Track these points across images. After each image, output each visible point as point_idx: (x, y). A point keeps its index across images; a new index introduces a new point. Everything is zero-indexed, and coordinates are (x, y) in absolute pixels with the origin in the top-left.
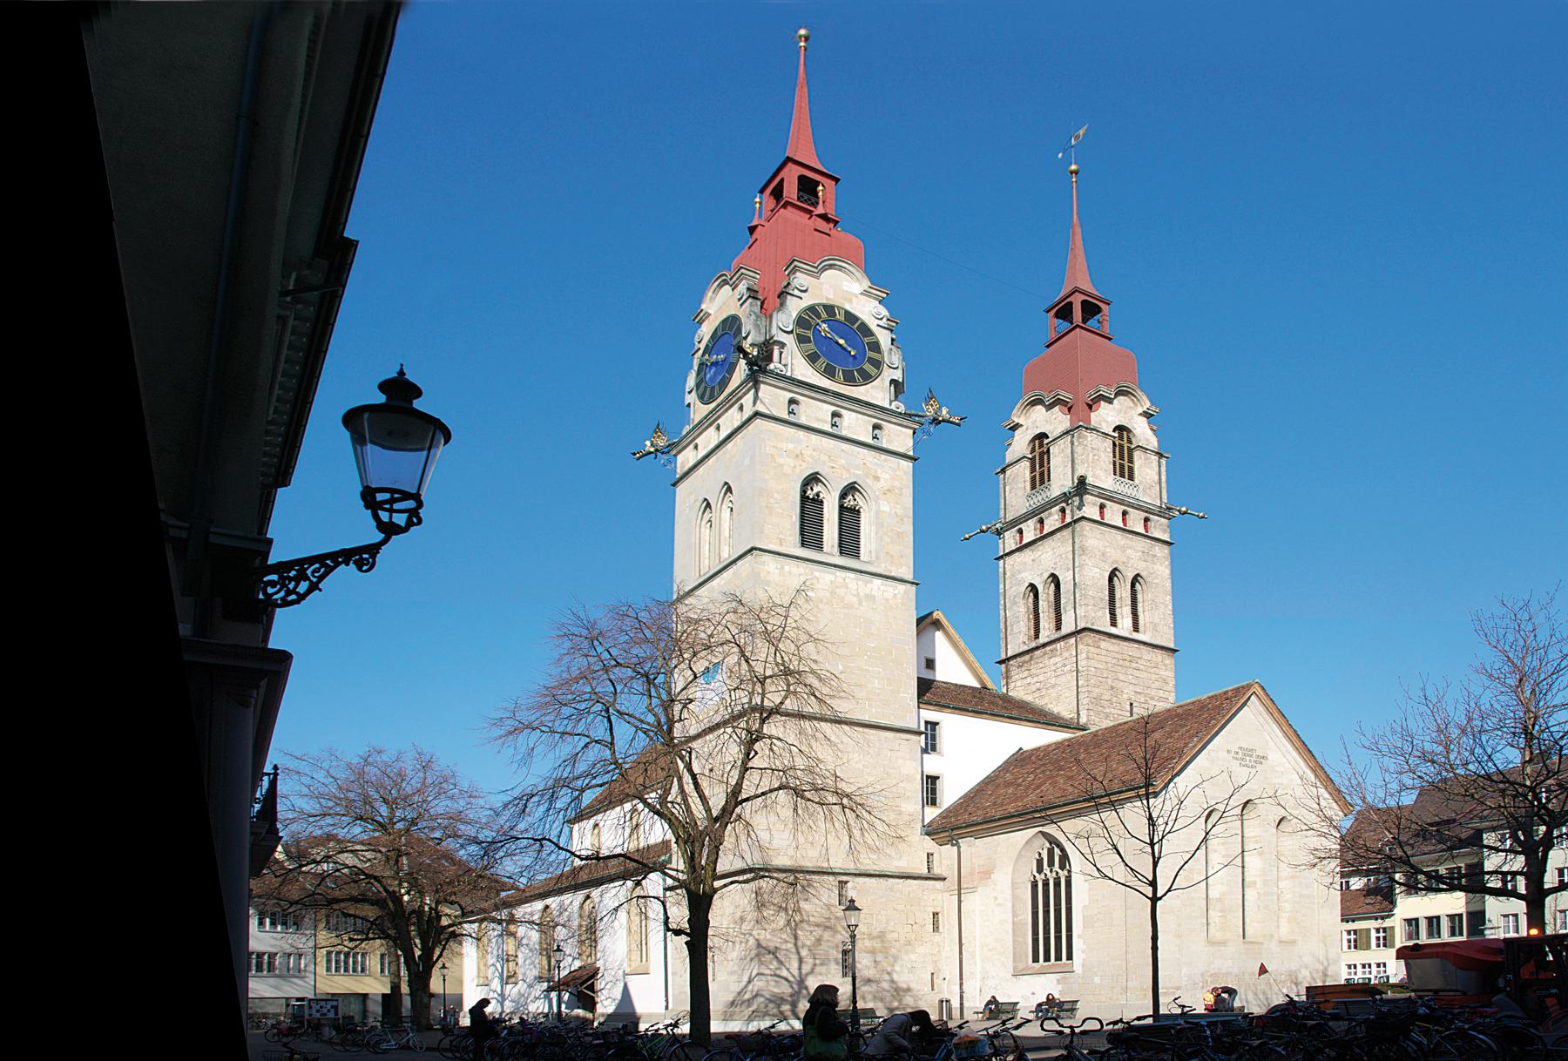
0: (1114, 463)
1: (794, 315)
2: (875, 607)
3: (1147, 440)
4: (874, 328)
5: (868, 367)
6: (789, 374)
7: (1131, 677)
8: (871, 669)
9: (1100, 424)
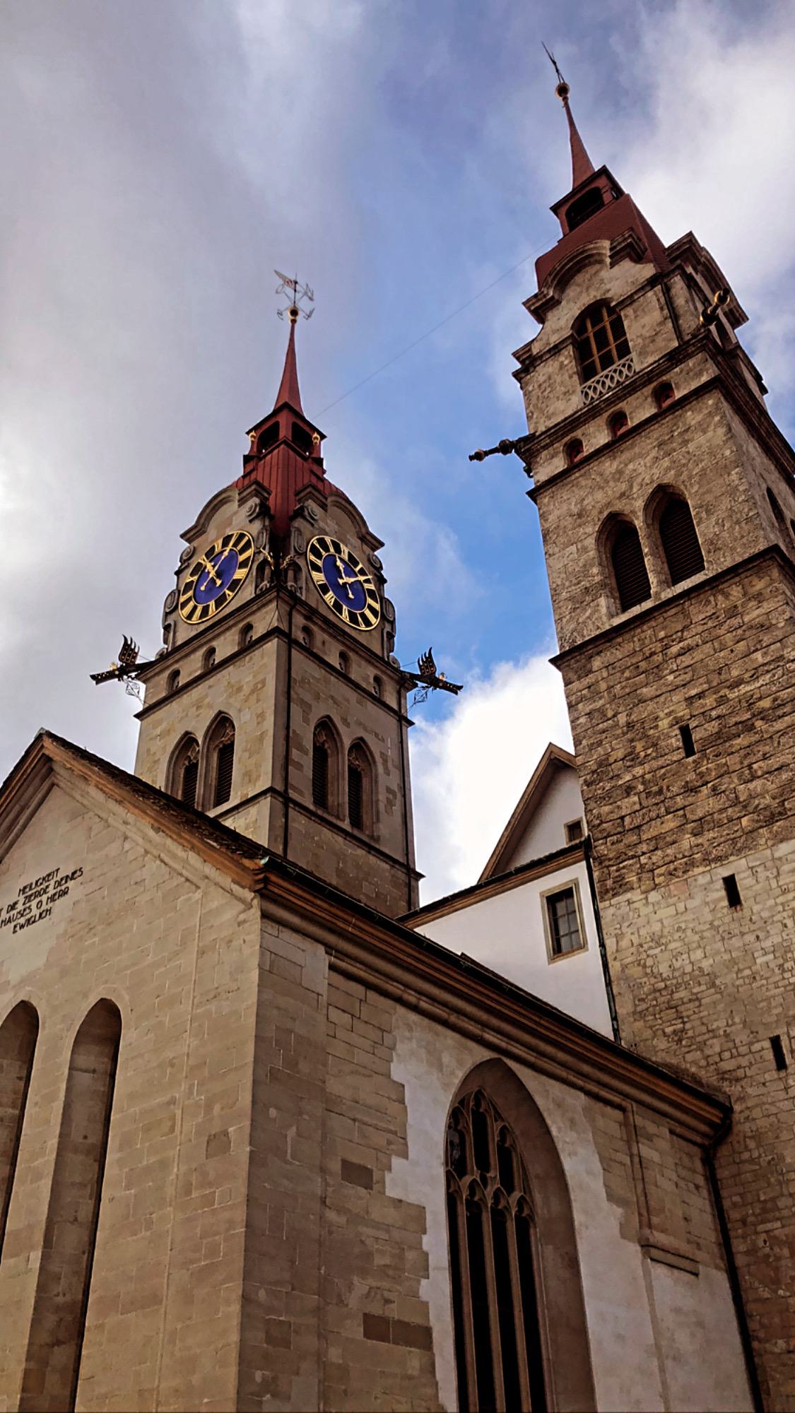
7: (671, 678)
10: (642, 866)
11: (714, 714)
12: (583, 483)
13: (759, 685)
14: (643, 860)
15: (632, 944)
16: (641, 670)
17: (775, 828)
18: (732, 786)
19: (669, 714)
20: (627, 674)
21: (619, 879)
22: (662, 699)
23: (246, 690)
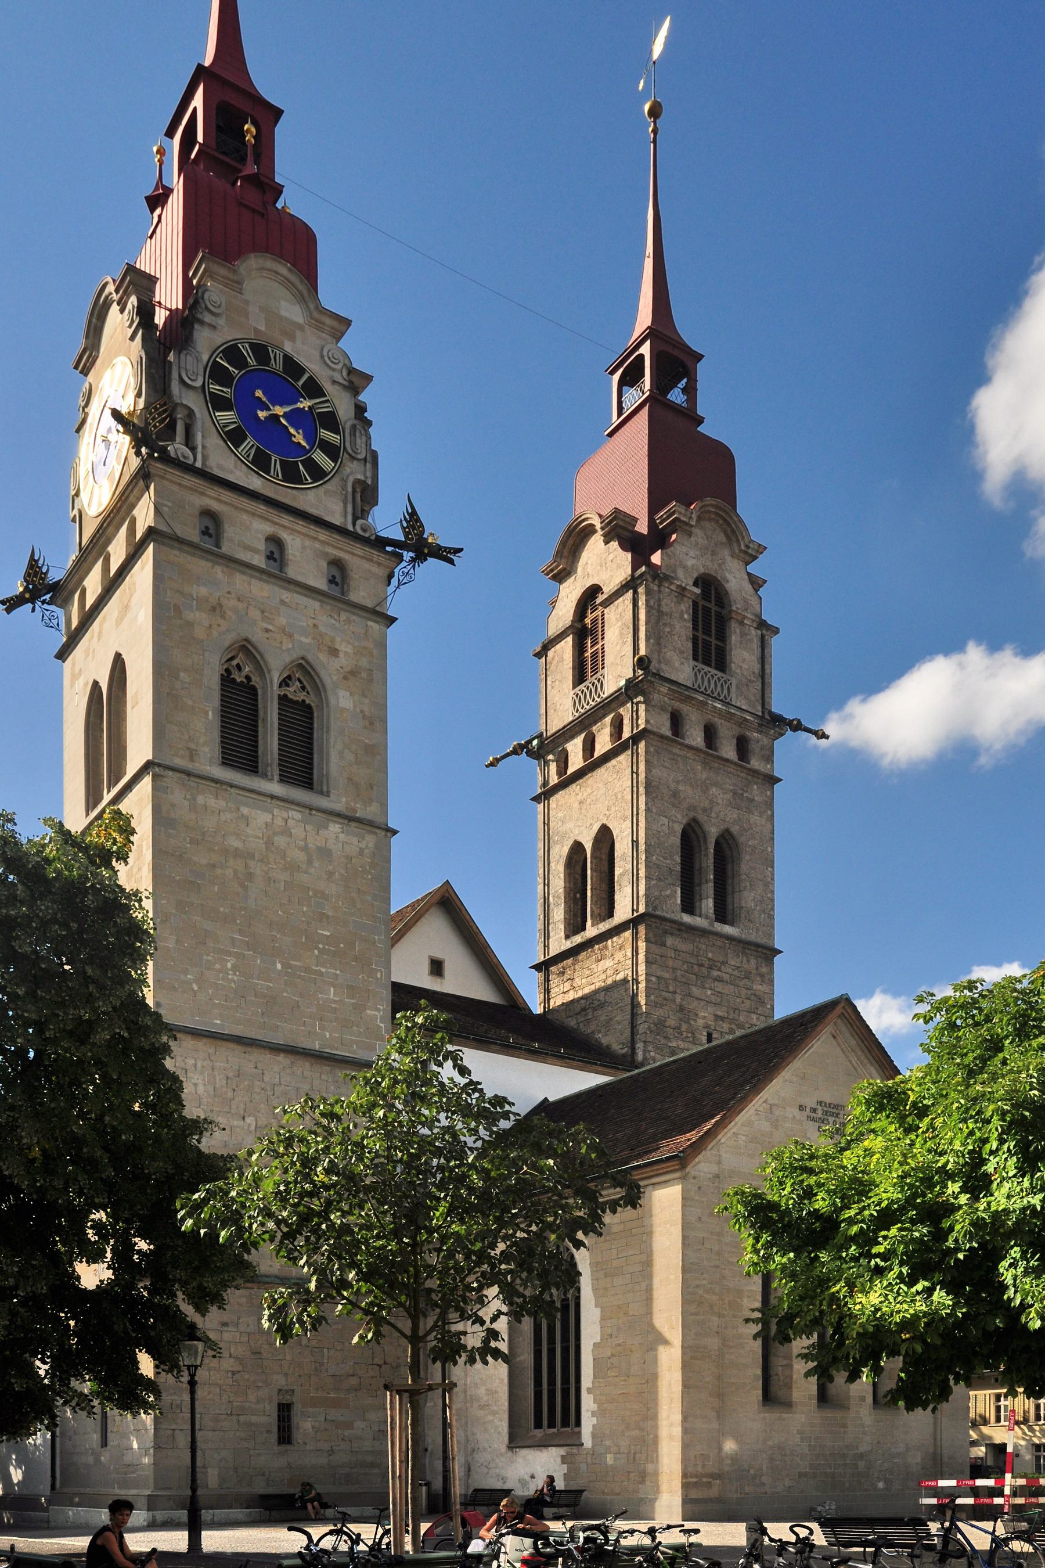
0: (695, 640)
1: (205, 357)
2: (331, 868)
3: (746, 601)
4: (327, 386)
5: (320, 458)
6: (199, 464)
7: (709, 992)
8: (323, 970)
9: (674, 571)
22: (702, 1003)
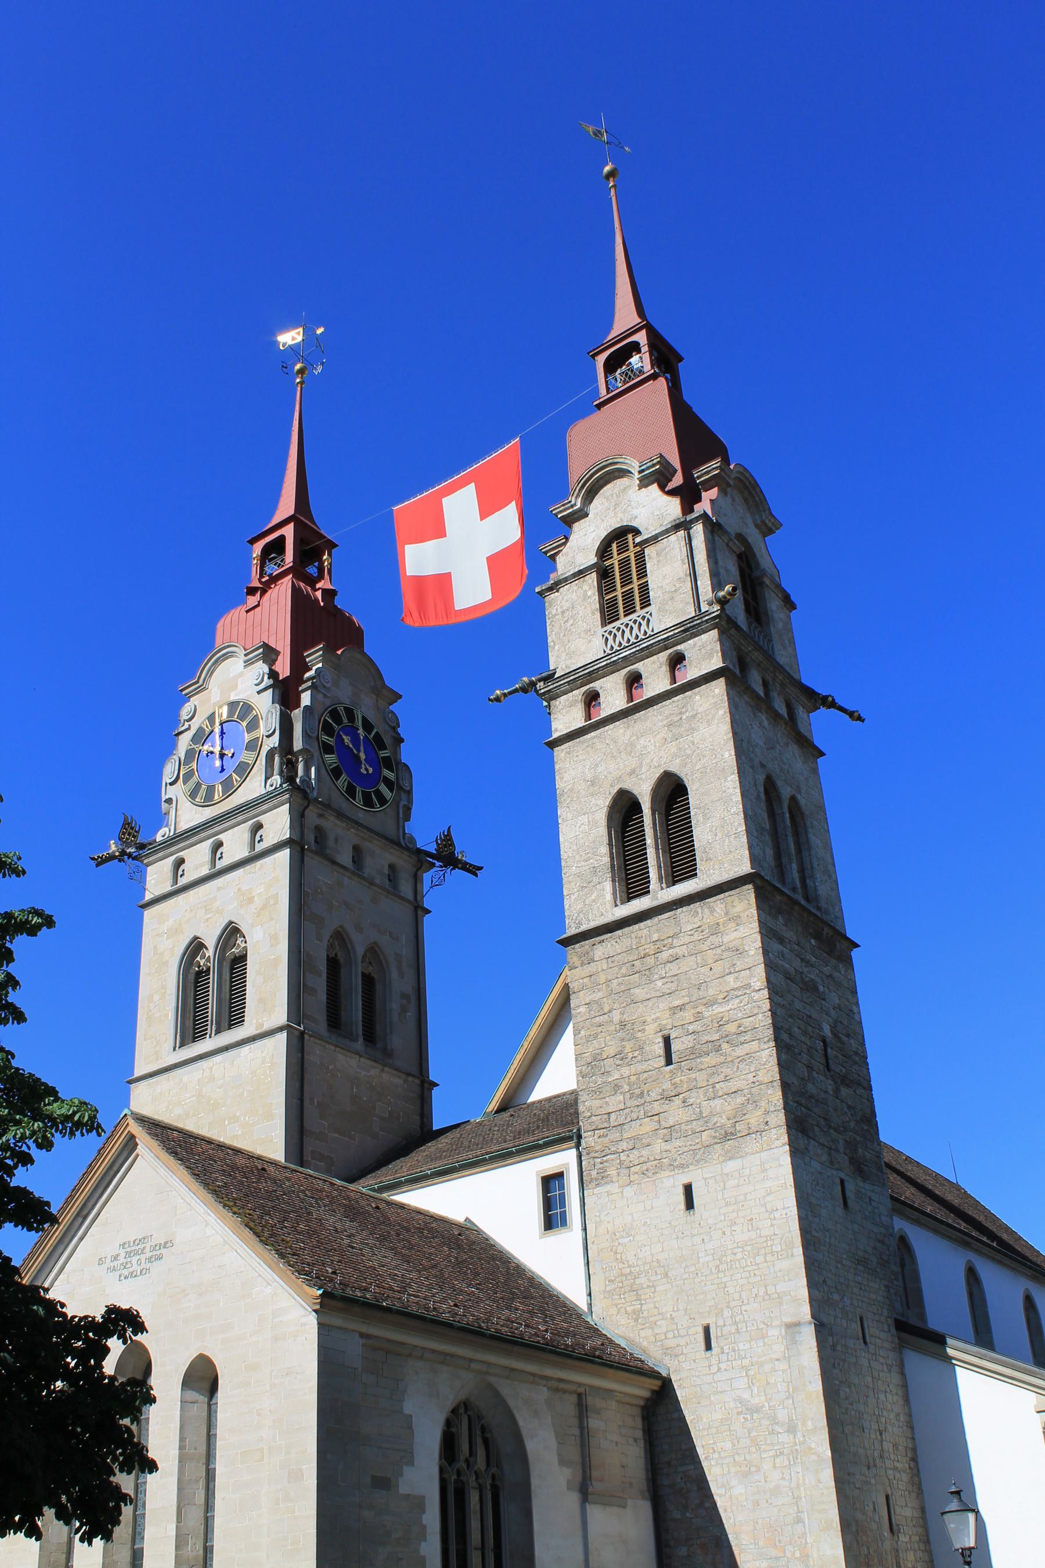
7: (659, 983)
10: (621, 1163)
11: (691, 1028)
12: (598, 746)
13: (728, 1008)
14: (623, 1157)
15: (608, 1232)
16: (636, 969)
17: (726, 1146)
18: (698, 1101)
19: (655, 1020)
20: (624, 970)
21: (602, 1171)
22: (650, 1003)
23: (258, 902)
